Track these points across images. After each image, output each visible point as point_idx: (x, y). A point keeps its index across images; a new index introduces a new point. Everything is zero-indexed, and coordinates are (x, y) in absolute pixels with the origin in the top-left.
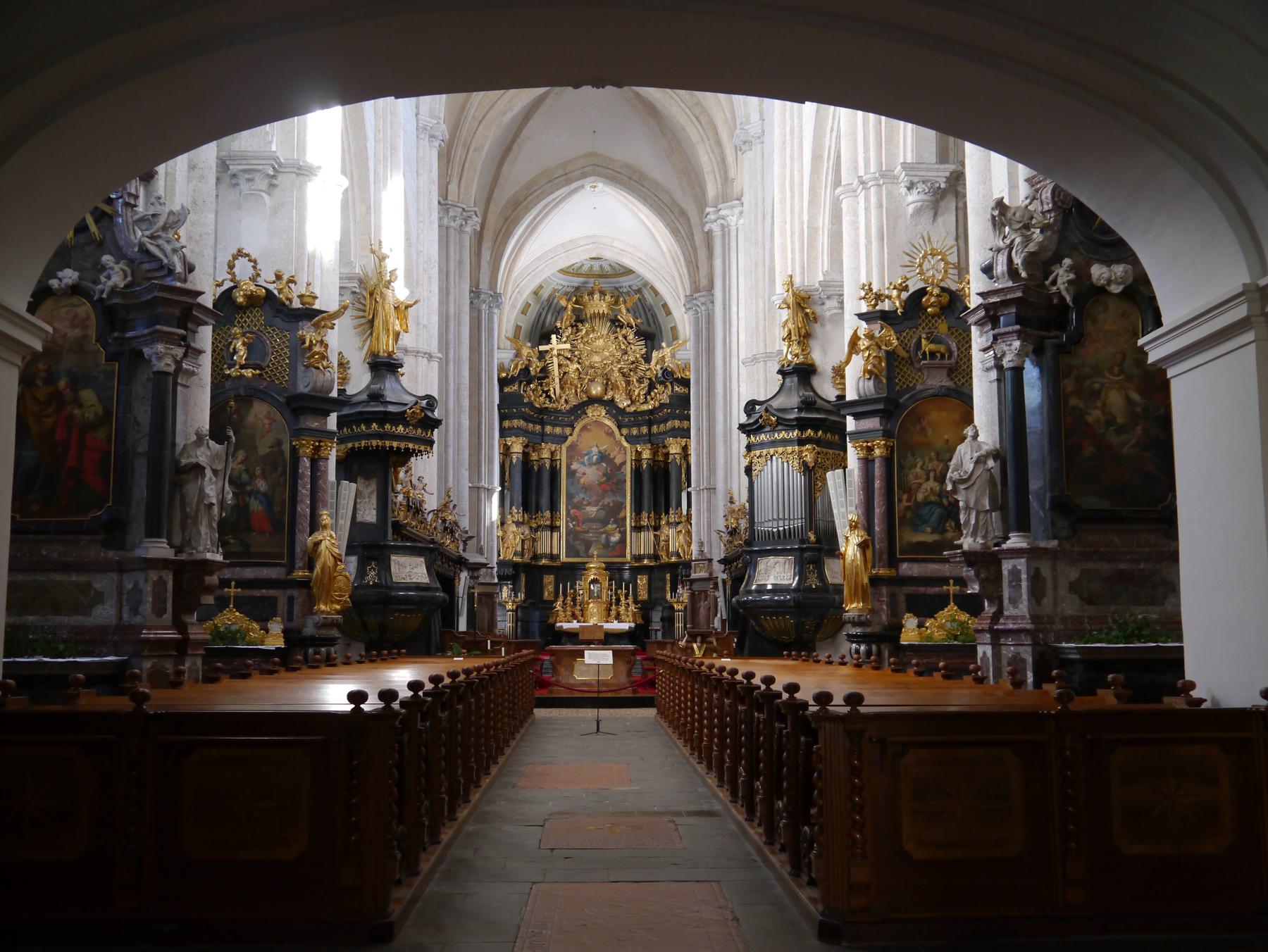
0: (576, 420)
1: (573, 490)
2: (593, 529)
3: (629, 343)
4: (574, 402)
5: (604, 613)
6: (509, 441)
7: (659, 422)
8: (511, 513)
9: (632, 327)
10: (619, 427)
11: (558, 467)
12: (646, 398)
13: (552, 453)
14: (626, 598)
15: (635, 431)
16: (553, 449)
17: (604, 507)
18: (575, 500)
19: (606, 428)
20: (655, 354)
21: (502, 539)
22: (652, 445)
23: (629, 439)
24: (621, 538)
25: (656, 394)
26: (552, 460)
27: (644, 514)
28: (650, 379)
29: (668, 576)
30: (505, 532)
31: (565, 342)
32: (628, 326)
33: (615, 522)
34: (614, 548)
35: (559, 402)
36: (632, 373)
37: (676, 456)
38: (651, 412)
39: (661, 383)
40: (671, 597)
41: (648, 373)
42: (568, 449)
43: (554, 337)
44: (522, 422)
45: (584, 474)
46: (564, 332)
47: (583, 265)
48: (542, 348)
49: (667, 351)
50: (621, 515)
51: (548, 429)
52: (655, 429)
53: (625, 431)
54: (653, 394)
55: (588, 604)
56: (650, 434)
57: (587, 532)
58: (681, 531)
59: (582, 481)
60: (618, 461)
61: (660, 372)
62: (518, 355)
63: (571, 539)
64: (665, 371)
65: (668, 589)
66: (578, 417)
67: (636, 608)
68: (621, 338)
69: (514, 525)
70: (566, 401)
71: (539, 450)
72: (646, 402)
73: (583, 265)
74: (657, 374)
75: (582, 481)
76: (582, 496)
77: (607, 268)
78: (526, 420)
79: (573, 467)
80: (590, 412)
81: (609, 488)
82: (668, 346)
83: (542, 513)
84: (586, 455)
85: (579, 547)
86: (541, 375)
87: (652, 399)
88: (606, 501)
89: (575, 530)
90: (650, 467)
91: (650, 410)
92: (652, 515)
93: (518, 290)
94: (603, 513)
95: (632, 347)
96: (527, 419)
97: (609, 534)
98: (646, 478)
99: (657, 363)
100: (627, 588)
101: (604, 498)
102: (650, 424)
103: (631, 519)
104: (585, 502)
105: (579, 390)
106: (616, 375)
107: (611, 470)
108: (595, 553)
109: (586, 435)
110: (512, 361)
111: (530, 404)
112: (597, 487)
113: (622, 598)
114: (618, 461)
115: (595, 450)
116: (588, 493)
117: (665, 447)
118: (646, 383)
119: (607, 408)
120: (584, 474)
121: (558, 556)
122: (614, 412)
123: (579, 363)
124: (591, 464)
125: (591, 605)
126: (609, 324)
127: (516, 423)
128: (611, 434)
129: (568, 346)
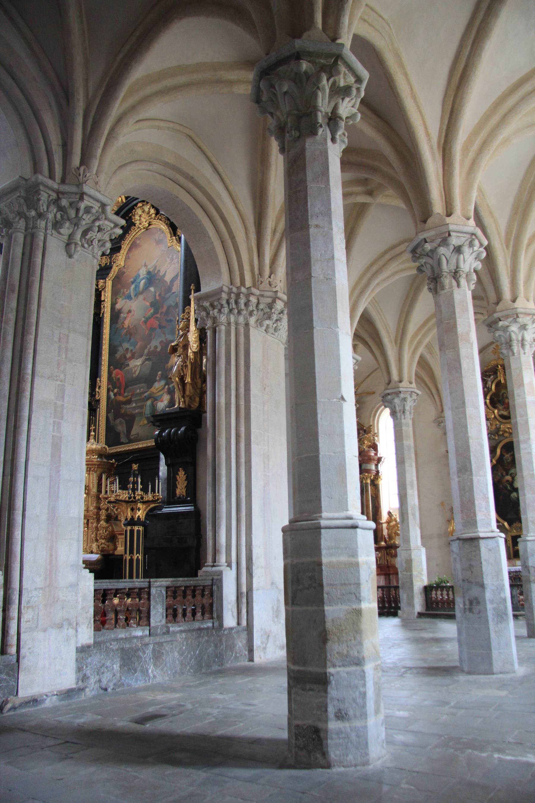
57: (129, 402)
63: (111, 416)
75: (127, 323)
79: (118, 306)
84: (133, 283)
97: (155, 399)
107: (160, 295)
120: (130, 311)
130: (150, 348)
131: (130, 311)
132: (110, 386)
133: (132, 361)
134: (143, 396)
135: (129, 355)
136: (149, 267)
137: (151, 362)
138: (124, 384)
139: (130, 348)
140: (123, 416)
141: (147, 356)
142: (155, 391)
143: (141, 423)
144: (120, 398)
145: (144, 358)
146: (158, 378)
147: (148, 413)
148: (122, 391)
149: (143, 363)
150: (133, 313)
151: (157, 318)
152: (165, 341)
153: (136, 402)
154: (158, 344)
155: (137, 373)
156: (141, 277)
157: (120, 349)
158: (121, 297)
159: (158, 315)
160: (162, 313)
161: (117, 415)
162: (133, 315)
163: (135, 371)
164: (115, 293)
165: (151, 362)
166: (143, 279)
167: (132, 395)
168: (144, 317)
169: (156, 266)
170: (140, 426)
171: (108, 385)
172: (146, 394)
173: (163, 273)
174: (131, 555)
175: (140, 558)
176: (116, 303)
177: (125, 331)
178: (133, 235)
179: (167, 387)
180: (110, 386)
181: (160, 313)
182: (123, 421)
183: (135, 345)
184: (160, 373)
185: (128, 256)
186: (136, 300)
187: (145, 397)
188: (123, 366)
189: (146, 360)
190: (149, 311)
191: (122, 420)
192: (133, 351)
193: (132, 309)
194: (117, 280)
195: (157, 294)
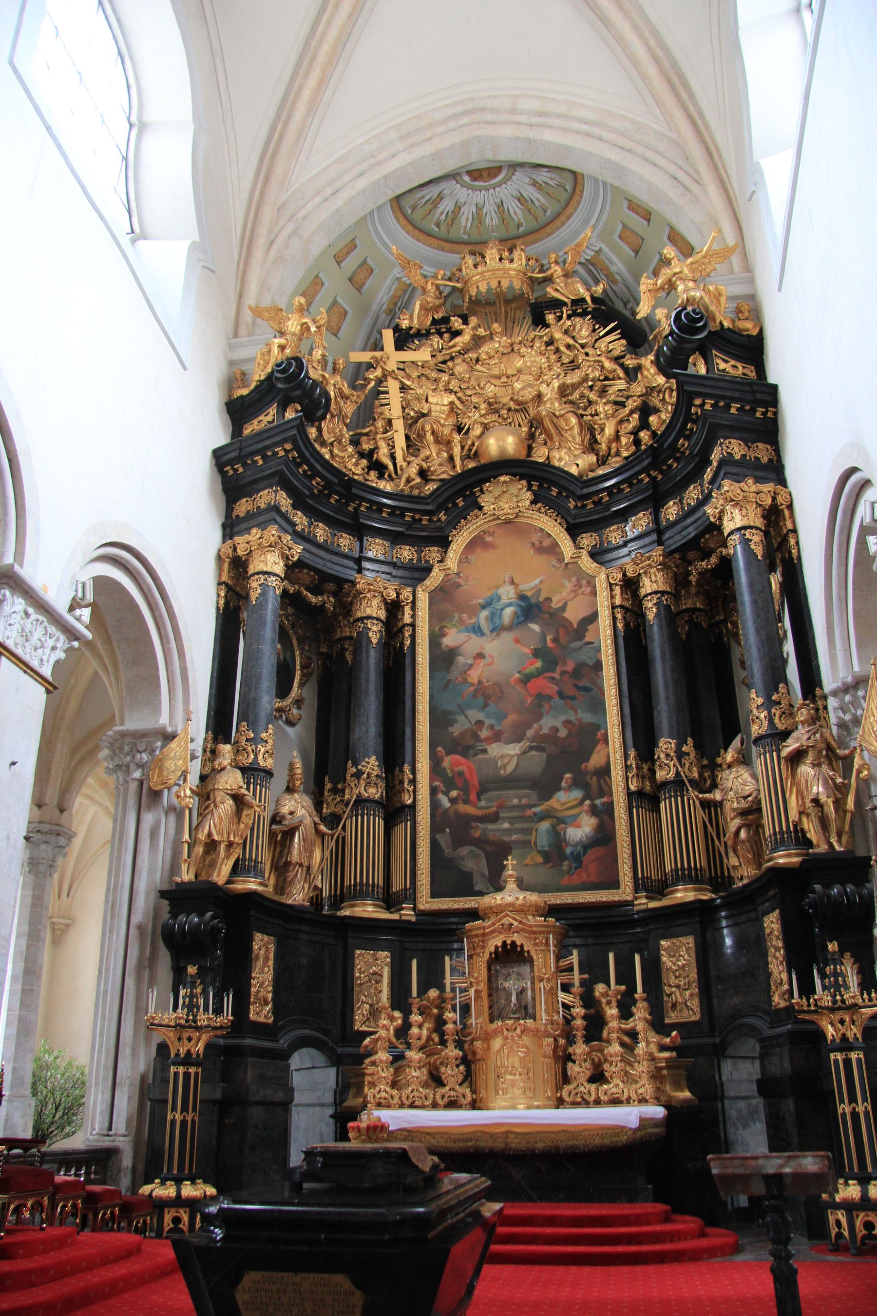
0: (453, 525)
1: (448, 704)
2: (513, 808)
4: (443, 472)
5: (545, 1066)
9: (584, 314)
10: (574, 531)
11: (408, 642)
13: (394, 608)
14: (626, 1013)
17: (540, 743)
18: (456, 730)
19: (536, 538)
27: (666, 745)
29: (772, 923)
32: (574, 314)
33: (576, 783)
34: (577, 858)
42: (433, 596)
45: (480, 656)
47: (458, 207)
50: (596, 760)
52: (671, 511)
53: (588, 540)
55: (487, 1038)
57: (494, 818)
58: (797, 757)
59: (474, 676)
60: (574, 614)
63: (444, 840)
65: (778, 968)
66: (459, 517)
67: (663, 1048)
69: (239, 774)
70: (423, 473)
73: (458, 207)
75: (474, 676)
76: (475, 715)
77: (516, 211)
80: (486, 500)
81: (556, 688)
83: (355, 764)
84: (484, 607)
85: (470, 865)
88: (547, 724)
89: (456, 813)
90: (669, 617)
92: (688, 747)
93: (291, 227)
94: (537, 759)
97: (559, 821)
100: (626, 976)
101: (540, 717)
103: (627, 768)
105: (457, 451)
106: (552, 405)
107: (555, 640)
109: (480, 557)
112: (519, 688)
114: (574, 614)
115: (508, 593)
116: (492, 707)
120: (480, 656)
121: (410, 894)
124: (498, 630)
125: (497, 1043)
126: (529, 320)
128: (553, 549)
130: (541, 728)
133: (494, 746)
134: (529, 813)
135: (484, 734)
136: (522, 587)
137: (544, 755)
138: (477, 784)
139: (488, 722)
140: (479, 843)
141: (532, 741)
142: (558, 807)
143: (528, 861)
145: (525, 744)
146: (563, 784)
147: (545, 843)
150: (488, 660)
151: (553, 678)
152: (576, 722)
153: (511, 820)
154: (558, 723)
155: (510, 769)
157: (461, 718)
158: (454, 626)
159: (556, 675)
160: (563, 673)
161: (461, 838)
163: (505, 766)
164: (438, 617)
165: (544, 755)
166: (510, 605)
167: (499, 807)
168: (519, 672)
169: (539, 591)
170: (525, 865)
171: (432, 780)
172: (537, 810)
173: (560, 605)
174: (853, 1105)
175: (869, 1108)
176: (444, 635)
177: (472, 689)
178: (478, 524)
179: (587, 802)
181: (558, 670)
182: (477, 851)
183: (501, 716)
184: (568, 775)
185: (466, 558)
186: (493, 639)
187: (535, 814)
188: (471, 752)
189: (531, 748)
190: (531, 664)
191: (474, 848)
192: (497, 728)
194: (439, 595)
195: (548, 638)
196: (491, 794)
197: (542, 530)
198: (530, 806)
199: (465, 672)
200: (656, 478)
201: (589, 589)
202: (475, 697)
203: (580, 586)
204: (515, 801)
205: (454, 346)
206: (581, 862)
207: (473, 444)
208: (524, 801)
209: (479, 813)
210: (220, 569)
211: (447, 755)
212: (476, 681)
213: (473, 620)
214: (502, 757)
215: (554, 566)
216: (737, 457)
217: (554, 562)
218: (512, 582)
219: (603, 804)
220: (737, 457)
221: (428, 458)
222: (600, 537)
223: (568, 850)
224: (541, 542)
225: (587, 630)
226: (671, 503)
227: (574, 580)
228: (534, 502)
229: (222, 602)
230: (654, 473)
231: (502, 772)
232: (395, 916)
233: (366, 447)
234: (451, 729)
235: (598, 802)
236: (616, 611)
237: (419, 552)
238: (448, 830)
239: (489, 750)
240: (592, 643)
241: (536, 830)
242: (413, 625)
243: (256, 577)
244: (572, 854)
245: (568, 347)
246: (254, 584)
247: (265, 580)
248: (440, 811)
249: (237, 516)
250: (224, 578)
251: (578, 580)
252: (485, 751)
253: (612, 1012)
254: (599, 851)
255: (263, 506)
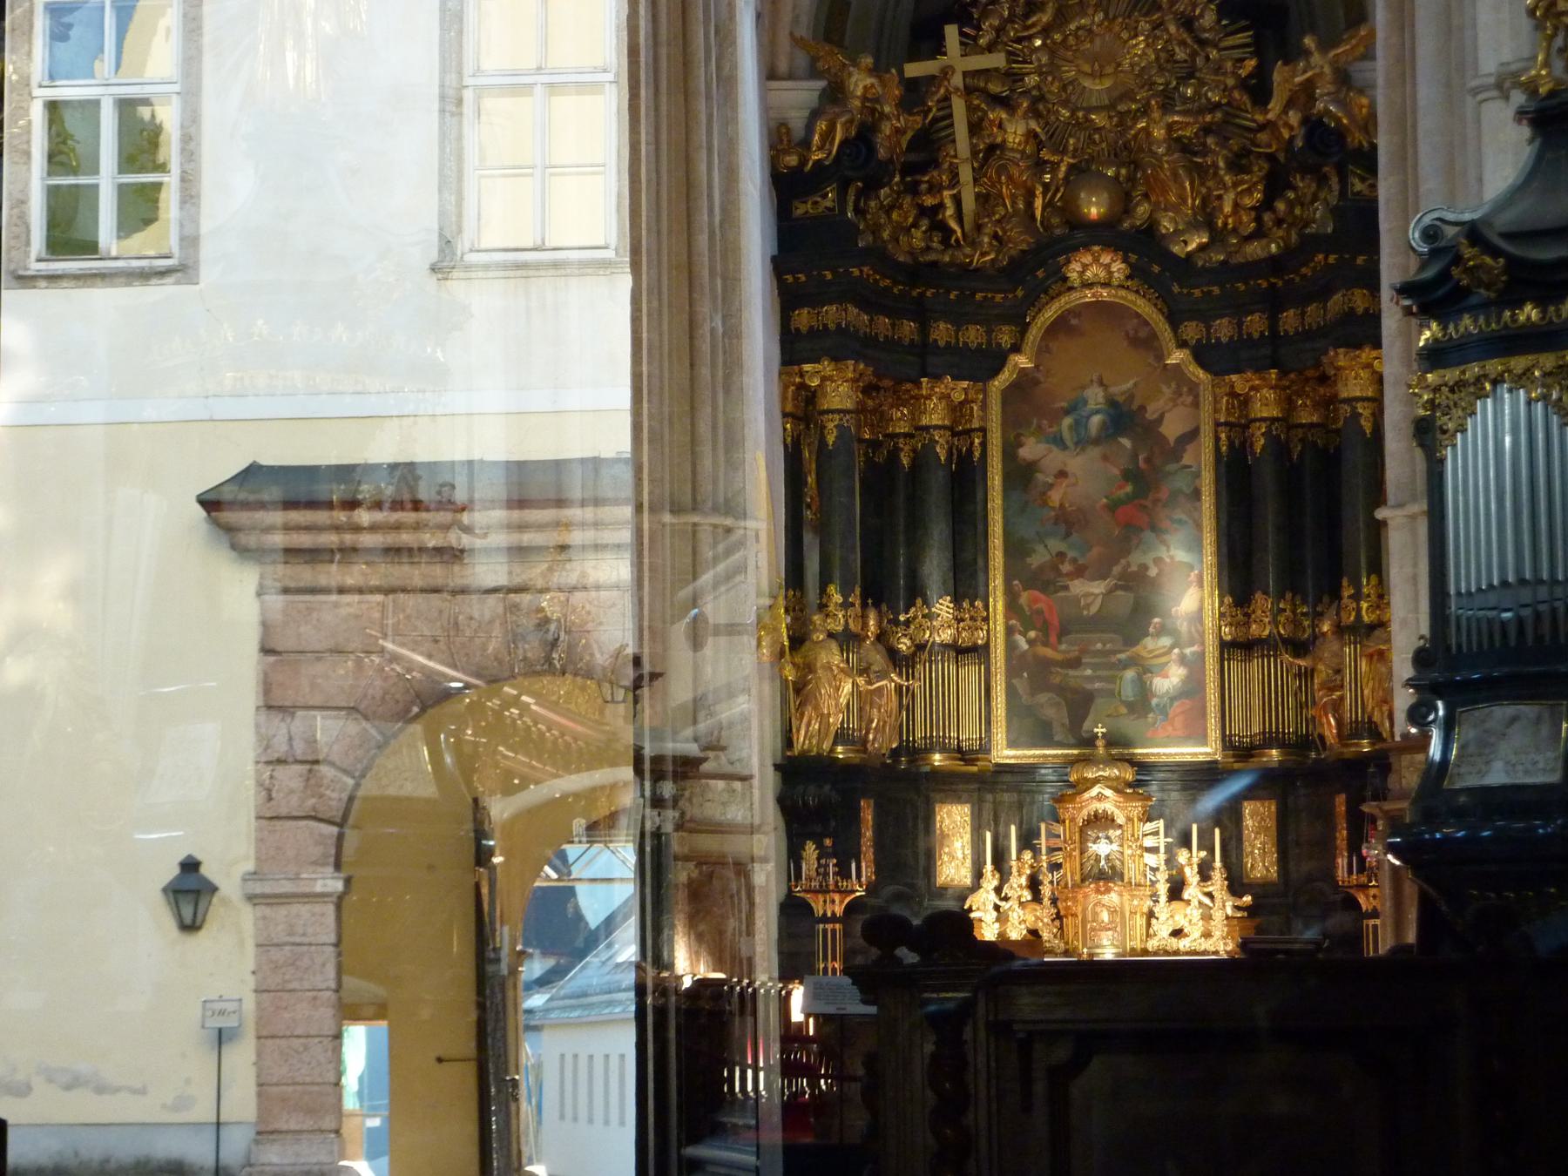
3: (1203, 43)
4: (1020, 241)
6: (814, 372)
7: (1302, 301)
8: (822, 607)
10: (1174, 320)
12: (1258, 220)
13: (958, 410)
15: (1223, 329)
16: (958, 397)
20: (1279, 74)
21: (798, 691)
22: (1284, 373)
23: (1203, 354)
24: (1187, 680)
25: (1291, 205)
26: (958, 429)
28: (1271, 158)
30: (808, 668)
31: (990, 48)
35: (974, 244)
36: (1210, 141)
37: (1360, 408)
38: (1274, 265)
39: (1305, 170)
40: (1350, 872)
41: (1263, 137)
43: (951, 32)
44: (853, 310)
46: (985, 14)
48: (913, 70)
49: (1319, 63)
51: (942, 332)
52: (1289, 320)
54: (1281, 206)
56: (1274, 336)
57: (1075, 663)
61: (1300, 133)
62: (835, 94)
63: (1021, 685)
64: (1315, 127)
66: (1038, 295)
67: (1237, 908)
68: (1172, 29)
69: (834, 646)
71: (916, 402)
72: (1259, 233)
74: (1292, 138)
75: (1055, 497)
76: (1056, 545)
78: (865, 305)
80: (1073, 271)
82: (1325, 46)
84: (1067, 412)
86: (912, 157)
87: (1279, 222)
90: (1278, 447)
91: (1272, 259)
95: (1214, 54)
96: (870, 301)
98: (1267, 482)
99: (1290, 104)
102: (1273, 304)
104: (1066, 568)
107: (1148, 460)
108: (1100, 730)
110: (815, 115)
111: (879, 256)
113: (1191, 875)
114: (1172, 429)
115: (1095, 397)
116: (1075, 537)
117: (1324, 379)
118: (1260, 169)
119: (1133, 258)
120: (1062, 474)
122: (1156, 269)
123: (1037, 115)
124: (1083, 443)
127: (831, 314)
129: (997, 60)
130: (1129, 565)
131: (1062, 474)
132: (1013, 622)
134: (1113, 659)
135: (1066, 568)
136: (1114, 390)
139: (1071, 554)
140: (1061, 690)
142: (1144, 654)
144: (1048, 652)
145: (1110, 582)
146: (1151, 630)
148: (1053, 639)
149: (1110, 592)
150: (1071, 480)
153: (1094, 667)
155: (1094, 609)
156: (1092, 406)
157: (1040, 548)
158: (1033, 434)
162: (1074, 485)
163: (1088, 606)
166: (1097, 412)
168: (1106, 497)
171: (1007, 617)
172: (1122, 656)
173: (1155, 416)
176: (1021, 445)
177: (1053, 513)
179: (1176, 651)
180: (1013, 622)
185: (1047, 346)
187: (1119, 661)
189: (1117, 587)
190: (1121, 487)
193: (1068, 469)
196: (1072, 637)
197: (1138, 315)
198: (1115, 652)
199: (1044, 493)
200: (1275, 284)
201: (1189, 399)
202: (1056, 523)
203: (1181, 395)
204: (1099, 646)
205: (1033, 25)
206: (1167, 715)
207: (1057, 190)
208: (1108, 646)
209: (1058, 657)
210: (784, 399)
211: (1025, 590)
212: (1057, 504)
213: (1054, 429)
214: (1087, 595)
215: (1150, 364)
216: (1360, 311)
217: (1151, 360)
218: (1101, 383)
219: (1193, 654)
220: (1360, 311)
221: (1004, 217)
222: (1208, 328)
223: (1154, 701)
224: (1136, 332)
225: (1184, 451)
226: (1291, 312)
227: (1173, 385)
228: (1128, 278)
229: (789, 439)
230: (1273, 280)
231: (1085, 613)
232: (975, 769)
233: (929, 201)
234: (1029, 560)
235: (1188, 651)
236: (1220, 429)
237: (989, 332)
238: (1025, 674)
239: (1072, 589)
240: (1190, 467)
241: (1121, 678)
242: (983, 430)
243: (831, 416)
244: (1157, 705)
245: (1183, 43)
246: (831, 425)
247: (841, 419)
248: (1017, 652)
249: (797, 330)
250: (789, 408)
251: (1178, 386)
252: (1066, 588)
253: (1191, 875)
254: (1187, 703)
255: (832, 326)
